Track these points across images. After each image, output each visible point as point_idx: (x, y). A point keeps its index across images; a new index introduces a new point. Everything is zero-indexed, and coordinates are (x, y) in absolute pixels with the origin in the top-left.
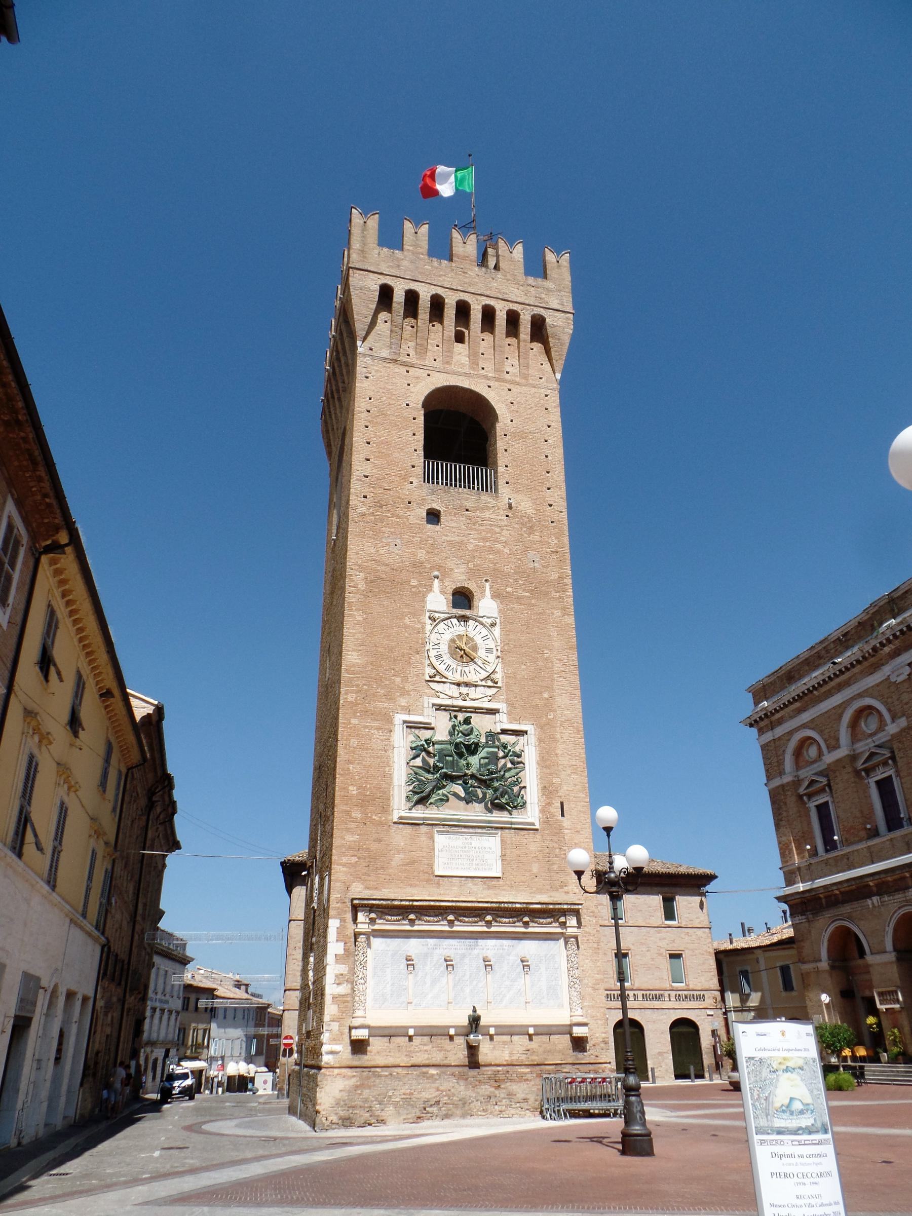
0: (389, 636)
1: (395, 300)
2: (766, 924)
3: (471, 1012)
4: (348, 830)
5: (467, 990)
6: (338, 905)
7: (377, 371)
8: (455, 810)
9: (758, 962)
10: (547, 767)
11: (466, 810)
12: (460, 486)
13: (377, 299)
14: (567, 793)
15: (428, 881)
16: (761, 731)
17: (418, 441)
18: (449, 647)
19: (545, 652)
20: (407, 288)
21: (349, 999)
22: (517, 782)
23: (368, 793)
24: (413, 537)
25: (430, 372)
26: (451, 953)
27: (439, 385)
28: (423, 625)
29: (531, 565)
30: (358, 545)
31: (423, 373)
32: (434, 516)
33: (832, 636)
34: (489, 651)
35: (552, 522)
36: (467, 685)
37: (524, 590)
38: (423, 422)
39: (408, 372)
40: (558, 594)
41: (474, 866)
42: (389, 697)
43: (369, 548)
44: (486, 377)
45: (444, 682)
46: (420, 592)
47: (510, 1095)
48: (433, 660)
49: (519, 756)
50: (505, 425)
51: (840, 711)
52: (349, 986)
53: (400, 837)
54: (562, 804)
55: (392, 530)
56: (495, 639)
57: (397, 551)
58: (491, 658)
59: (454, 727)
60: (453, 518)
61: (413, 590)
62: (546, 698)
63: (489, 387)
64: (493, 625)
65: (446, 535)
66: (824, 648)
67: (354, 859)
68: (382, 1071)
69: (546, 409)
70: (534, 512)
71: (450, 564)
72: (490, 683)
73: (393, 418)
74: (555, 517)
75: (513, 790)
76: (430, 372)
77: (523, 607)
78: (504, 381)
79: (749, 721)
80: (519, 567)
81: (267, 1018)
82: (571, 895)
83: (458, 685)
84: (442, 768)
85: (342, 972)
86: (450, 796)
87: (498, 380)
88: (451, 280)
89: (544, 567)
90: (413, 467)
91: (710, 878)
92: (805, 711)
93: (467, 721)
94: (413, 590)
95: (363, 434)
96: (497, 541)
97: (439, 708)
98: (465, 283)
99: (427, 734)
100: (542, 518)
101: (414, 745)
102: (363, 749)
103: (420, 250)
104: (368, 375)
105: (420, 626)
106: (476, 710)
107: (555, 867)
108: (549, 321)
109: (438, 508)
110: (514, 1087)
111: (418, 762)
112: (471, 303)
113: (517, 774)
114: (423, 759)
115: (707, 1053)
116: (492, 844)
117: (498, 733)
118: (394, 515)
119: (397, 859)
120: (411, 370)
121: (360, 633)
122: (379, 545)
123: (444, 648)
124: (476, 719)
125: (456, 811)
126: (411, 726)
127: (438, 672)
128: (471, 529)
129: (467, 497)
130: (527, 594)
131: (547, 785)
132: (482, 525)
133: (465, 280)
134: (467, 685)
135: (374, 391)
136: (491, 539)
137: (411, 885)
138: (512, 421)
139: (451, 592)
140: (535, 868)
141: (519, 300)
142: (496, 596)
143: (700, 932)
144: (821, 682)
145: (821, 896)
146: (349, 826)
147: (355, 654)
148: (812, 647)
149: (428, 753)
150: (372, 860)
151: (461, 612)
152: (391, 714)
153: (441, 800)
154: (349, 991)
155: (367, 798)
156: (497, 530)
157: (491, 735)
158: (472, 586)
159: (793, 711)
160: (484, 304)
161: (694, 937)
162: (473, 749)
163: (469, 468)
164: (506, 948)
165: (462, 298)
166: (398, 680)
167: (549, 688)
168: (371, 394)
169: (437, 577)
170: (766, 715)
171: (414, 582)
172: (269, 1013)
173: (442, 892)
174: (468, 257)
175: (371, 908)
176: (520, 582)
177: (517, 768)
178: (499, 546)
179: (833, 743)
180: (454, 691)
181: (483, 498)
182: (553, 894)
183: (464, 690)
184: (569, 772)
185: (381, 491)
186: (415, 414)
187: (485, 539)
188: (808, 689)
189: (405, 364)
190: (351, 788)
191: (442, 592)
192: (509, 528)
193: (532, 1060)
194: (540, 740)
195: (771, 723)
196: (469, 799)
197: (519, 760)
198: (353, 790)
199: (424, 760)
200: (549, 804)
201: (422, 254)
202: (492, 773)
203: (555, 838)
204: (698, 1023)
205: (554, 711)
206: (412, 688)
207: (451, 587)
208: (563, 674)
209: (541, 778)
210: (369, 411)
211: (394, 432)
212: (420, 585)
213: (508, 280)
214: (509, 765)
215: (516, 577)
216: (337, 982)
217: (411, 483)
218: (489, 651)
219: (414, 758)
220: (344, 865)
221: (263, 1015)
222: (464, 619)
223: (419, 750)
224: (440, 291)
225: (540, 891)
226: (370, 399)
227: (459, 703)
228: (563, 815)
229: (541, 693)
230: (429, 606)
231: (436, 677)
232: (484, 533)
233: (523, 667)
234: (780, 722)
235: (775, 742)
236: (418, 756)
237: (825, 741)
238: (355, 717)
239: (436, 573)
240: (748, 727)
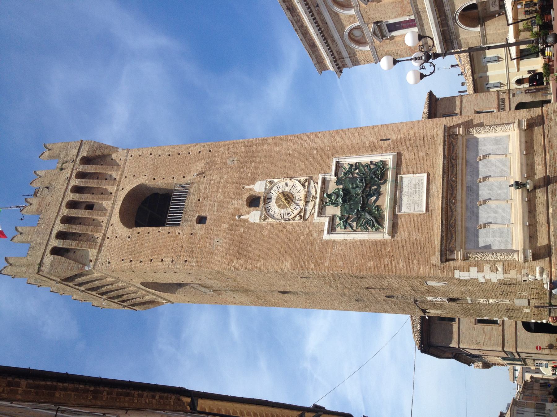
0: (275, 244)
1: (61, 246)
2: (459, 75)
3: (513, 188)
4: (396, 266)
5: (499, 191)
6: (445, 272)
7: (106, 256)
8: (385, 203)
9: (482, 77)
10: (359, 149)
11: (385, 196)
12: (184, 205)
13: (59, 257)
14: (375, 137)
15: (430, 217)
16: (345, 66)
17: (153, 230)
18: (283, 208)
19: (288, 153)
20: (55, 238)
21: (506, 263)
22: (368, 166)
23: (373, 254)
24: (213, 231)
25: (110, 225)
27: (119, 219)
28: (268, 224)
29: (235, 162)
30: (216, 264)
31: (110, 227)
33: (289, 17)
35: (210, 151)
37: (250, 166)
38: (141, 228)
39: (108, 238)
40: (254, 147)
41: (420, 189)
43: (218, 258)
44: (117, 191)
45: (305, 211)
46: (248, 226)
48: (290, 217)
49: (352, 165)
50: (148, 179)
51: (334, 14)
52: (498, 263)
53: (401, 234)
54: (381, 140)
55: (208, 244)
56: (280, 182)
57: (221, 241)
58: (291, 183)
59: (332, 204)
60: (203, 208)
61: (246, 230)
62: (317, 151)
63: (123, 189)
65: (214, 212)
66: (296, 23)
67: (415, 262)
68: (552, 241)
69: (140, 156)
70: (203, 162)
71: (231, 209)
72: (306, 184)
73: (137, 246)
74: (207, 149)
75: (373, 169)
76: (110, 225)
77: (261, 167)
78: (120, 180)
79: (339, 72)
80: (236, 169)
81: (523, 401)
82: (439, 132)
84: (358, 210)
85: (489, 268)
86: (375, 205)
87: (119, 185)
88: (52, 212)
89: (237, 155)
90: (169, 233)
91: (431, 94)
92: (333, 37)
93: (329, 196)
94: (246, 230)
95: (145, 263)
96: (219, 182)
97: (321, 213)
98: (56, 204)
100: (207, 156)
101: (343, 227)
102: (345, 258)
103: (32, 231)
104: (107, 262)
105: (269, 226)
107: (421, 142)
108: (85, 154)
109: (196, 217)
112: (69, 199)
113: (362, 166)
114: (352, 221)
115: (535, 98)
117: (337, 177)
118: (199, 243)
119: (415, 236)
120: (107, 235)
121: (271, 262)
122: (217, 252)
123: (283, 211)
125: (385, 201)
126: (332, 229)
127: (298, 214)
128: (211, 197)
129: (191, 201)
130: (253, 164)
131: (370, 149)
132: (209, 192)
133: (54, 203)
135: (118, 258)
136: (218, 185)
137: (433, 227)
138: (145, 176)
139: (248, 209)
140: (421, 154)
141: (70, 172)
142: (253, 182)
143: (464, 101)
144: (317, 25)
145: (442, 30)
146: (394, 265)
147: (284, 265)
148: (296, 30)
149: (348, 218)
150: (416, 251)
151: (262, 202)
152: (323, 241)
153: (378, 210)
154: (501, 263)
155: (376, 255)
156: (212, 182)
157: (338, 182)
158: (246, 196)
159: (333, 45)
160: (70, 192)
161: (466, 104)
163: (173, 200)
164: (472, 169)
165: (65, 205)
166: (302, 238)
168: (120, 260)
169: (239, 217)
170: (335, 61)
171: (242, 230)
172: (519, 400)
173: (437, 208)
174: (40, 202)
176: (245, 168)
177: (359, 166)
178: (222, 181)
179: (352, 19)
180: (311, 205)
181: (192, 191)
182: (438, 143)
184: (362, 137)
185: (183, 252)
186: (135, 233)
187: (218, 189)
188: (321, 33)
189: (103, 239)
190: (369, 265)
191: (249, 213)
192: (212, 176)
193: (542, 152)
194: (342, 154)
195: (339, 59)
197: (354, 165)
199: (353, 221)
200: (382, 148)
201: (34, 230)
202: (362, 180)
203: (403, 143)
204: (518, 102)
205: (325, 146)
206: (307, 230)
207: (245, 208)
208: (303, 142)
209: (366, 153)
210: (131, 261)
211: (146, 245)
212: (243, 226)
213: (57, 178)
214: (357, 171)
215: (242, 171)
216: (495, 271)
217: (179, 233)
218: (286, 185)
219: (352, 228)
220: (419, 268)
221: (520, 403)
222: (267, 200)
223: (346, 224)
224: (59, 218)
225: (436, 151)
226: (123, 260)
227: (317, 201)
228: (389, 139)
229: (313, 154)
230: (257, 221)
231: (302, 215)
232: (214, 190)
233: (297, 165)
234: (339, 53)
235: (351, 57)
236: (350, 225)
237: (351, 23)
238: (324, 263)
239: (237, 217)
240: (342, 74)
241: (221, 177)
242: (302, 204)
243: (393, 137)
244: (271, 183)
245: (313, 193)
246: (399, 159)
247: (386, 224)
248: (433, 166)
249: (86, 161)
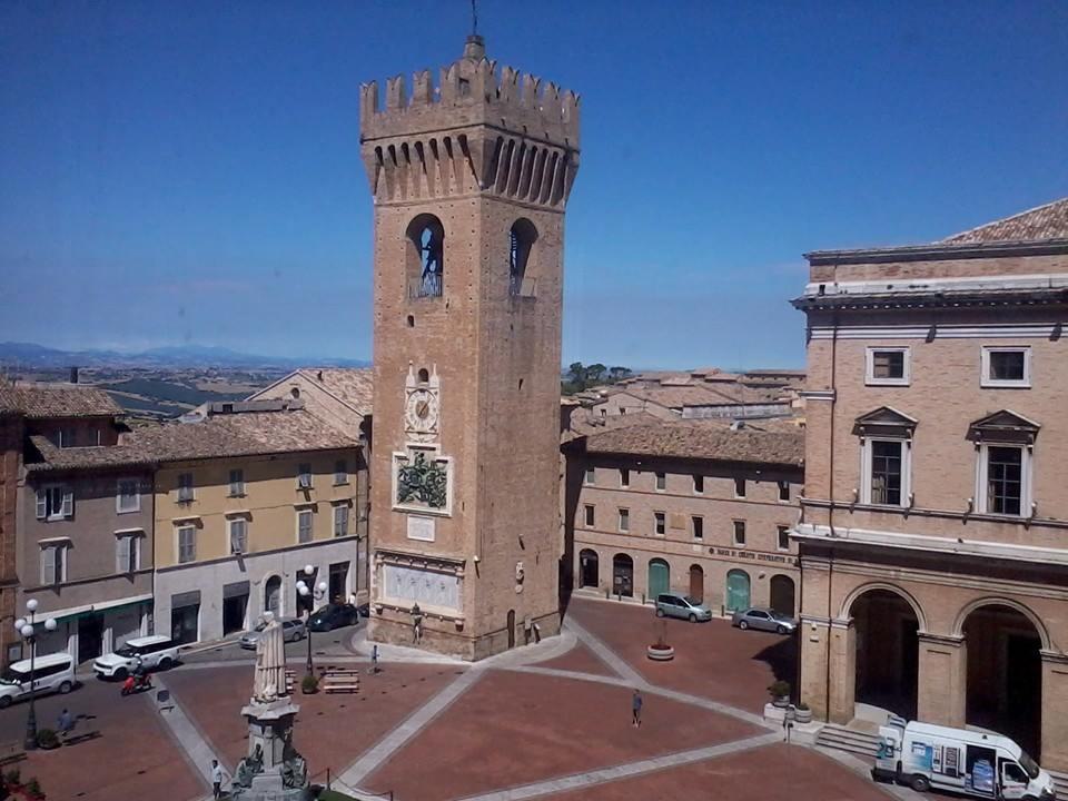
22: (442, 491)
26: (415, 577)
29: (457, 347)
34: (434, 410)
36: (423, 433)
42: (391, 443)
44: (438, 200)
47: (432, 643)
49: (445, 474)
64: (436, 393)
71: (418, 354)
83: (419, 433)
93: (422, 455)
97: (411, 447)
99: (405, 463)
110: (434, 640)
111: (402, 478)
116: (431, 523)
124: (426, 453)
134: (423, 433)
140: (449, 538)
157: (434, 463)
158: (427, 367)
162: (423, 472)
167: (463, 433)
175: (382, 553)
180: (416, 437)
183: (422, 436)
187: (435, 333)
191: (414, 374)
194: (456, 465)
198: (377, 493)
223: (402, 471)
231: (410, 430)
241: (445, 334)
242: (417, 428)
243: (465, 515)
244: (436, 393)
245: (427, 438)
246: (447, 517)
247: (401, 507)
248: (440, 548)
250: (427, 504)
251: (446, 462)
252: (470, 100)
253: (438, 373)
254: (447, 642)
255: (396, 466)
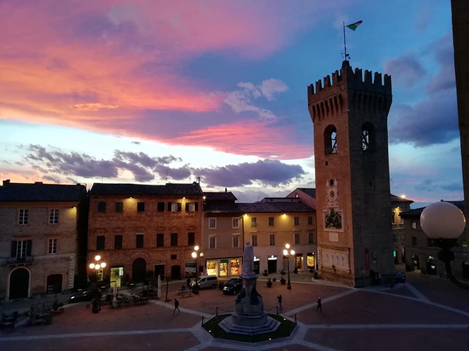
32: (327, 164)
93: (333, 210)
106: (335, 208)
108: (342, 95)
157: (337, 213)
162: (334, 216)
196: (334, 226)
207: (330, 179)
223: (326, 217)
249: (340, 96)
250: (335, 228)
251: (340, 212)
252: (342, 82)
253: (337, 180)
254: (345, 279)
255: (324, 216)
